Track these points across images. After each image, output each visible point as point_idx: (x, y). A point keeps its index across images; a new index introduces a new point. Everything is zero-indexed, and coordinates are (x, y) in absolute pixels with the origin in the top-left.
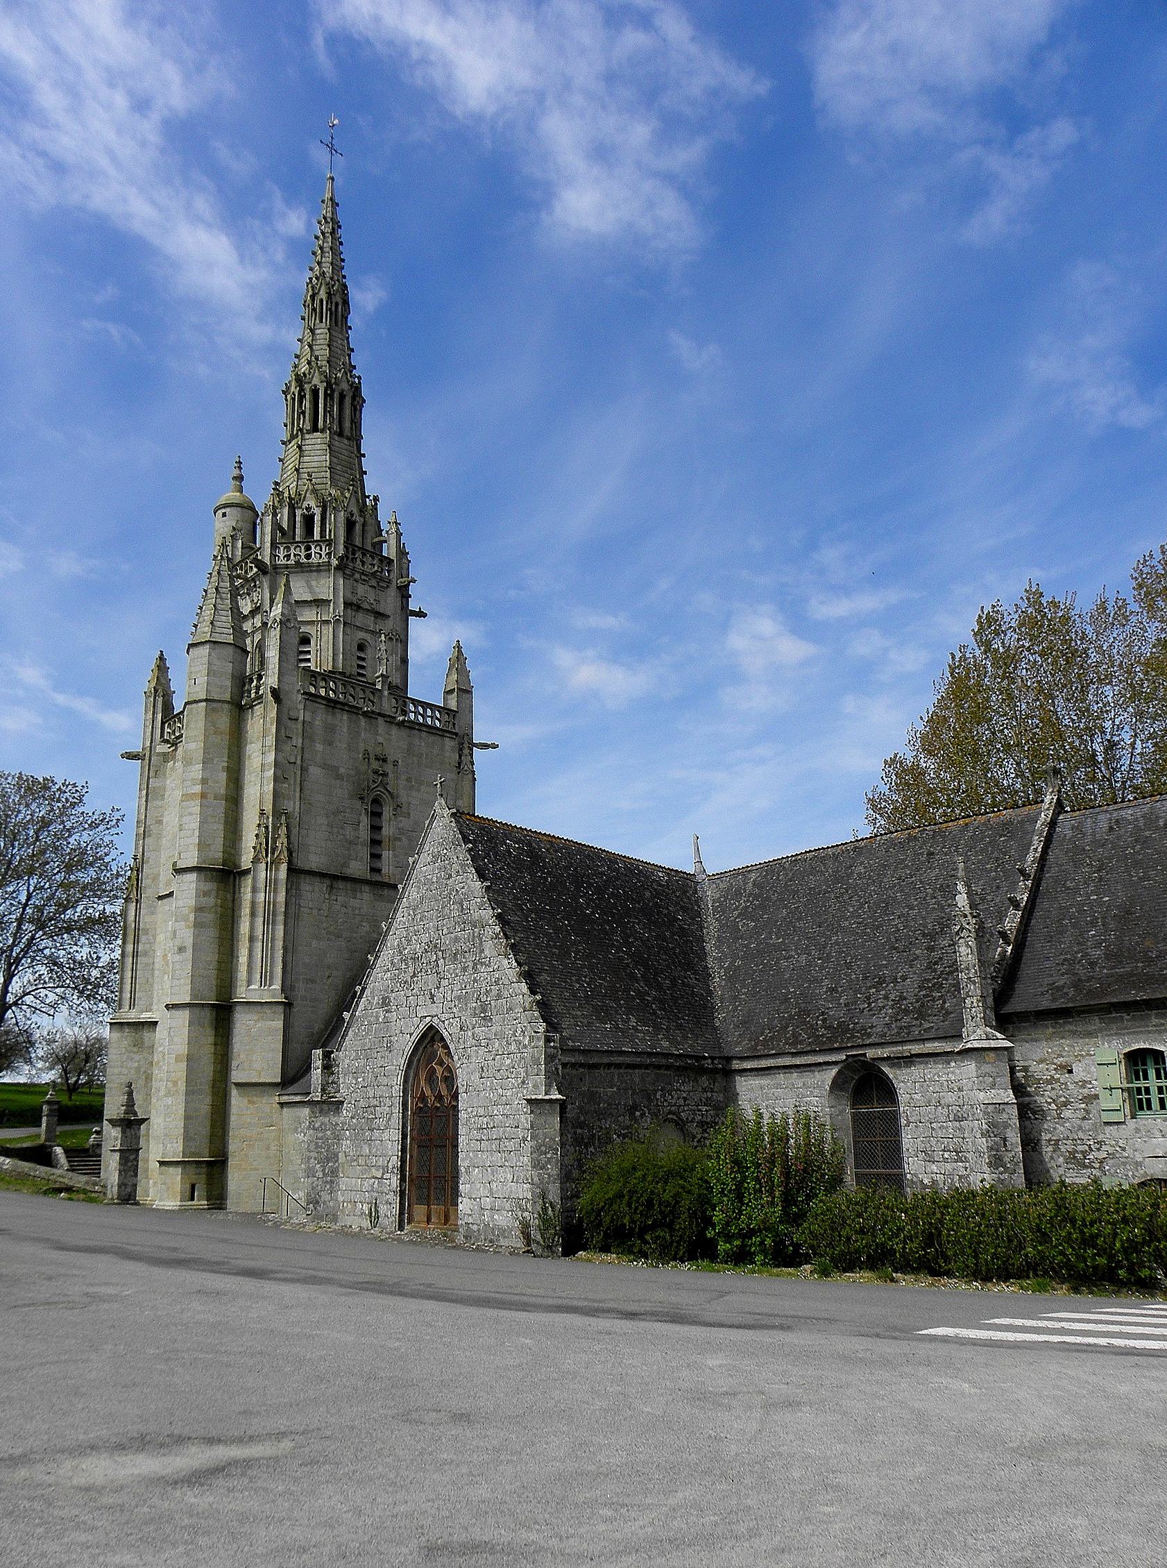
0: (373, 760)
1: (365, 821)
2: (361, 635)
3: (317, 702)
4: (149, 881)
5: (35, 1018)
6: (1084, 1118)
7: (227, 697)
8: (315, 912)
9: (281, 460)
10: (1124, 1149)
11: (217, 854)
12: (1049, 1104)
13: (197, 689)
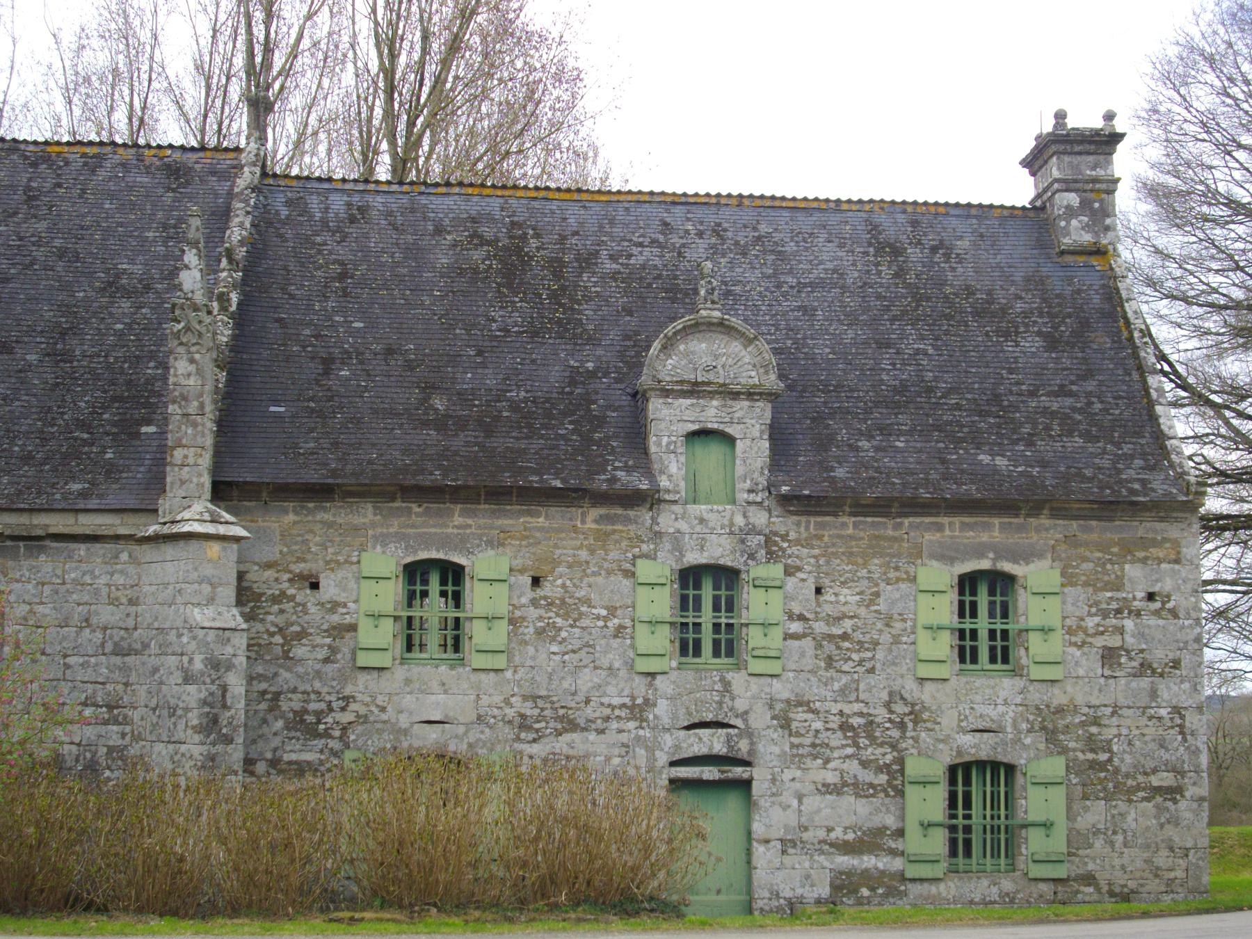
6: (327, 660)
10: (383, 709)
12: (272, 635)
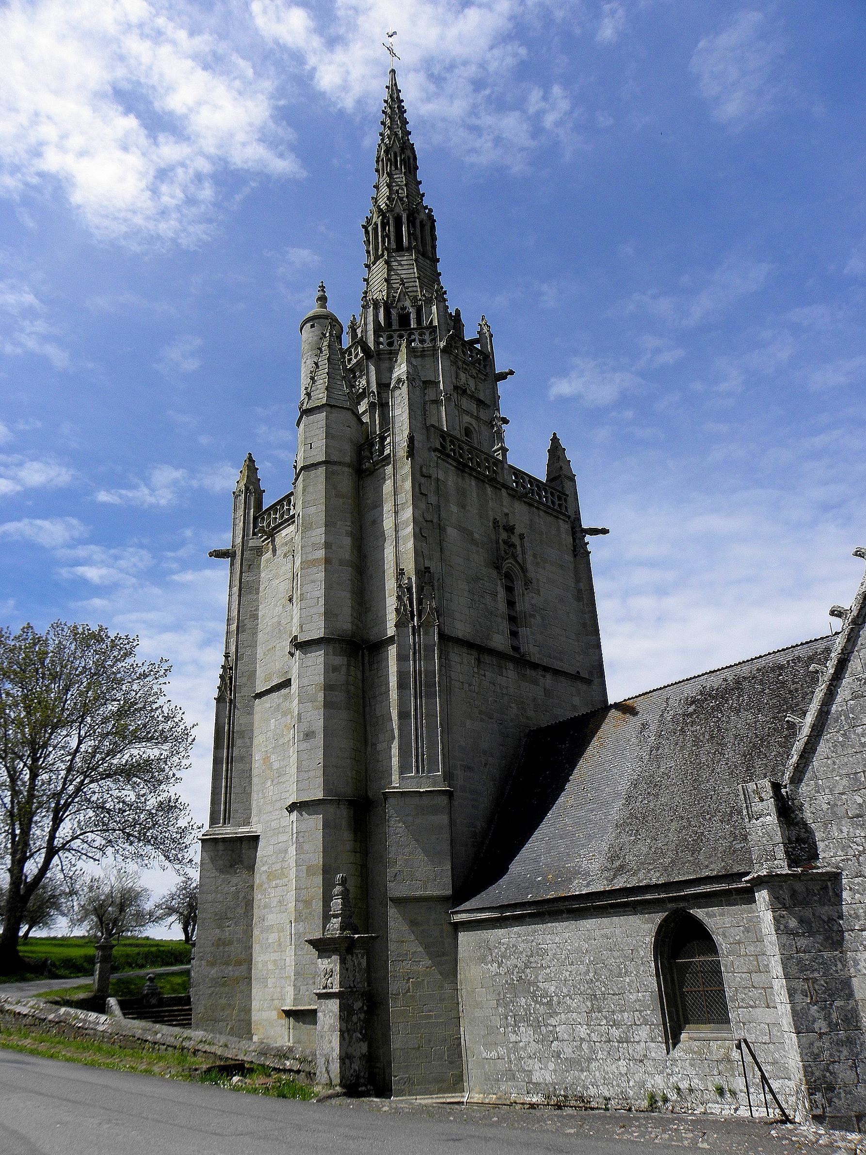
0: (501, 530)
1: (501, 593)
2: (467, 419)
3: (448, 463)
4: (244, 680)
5: (80, 864)
7: (347, 459)
8: (466, 686)
9: (365, 280)
11: (345, 624)
13: (313, 452)
